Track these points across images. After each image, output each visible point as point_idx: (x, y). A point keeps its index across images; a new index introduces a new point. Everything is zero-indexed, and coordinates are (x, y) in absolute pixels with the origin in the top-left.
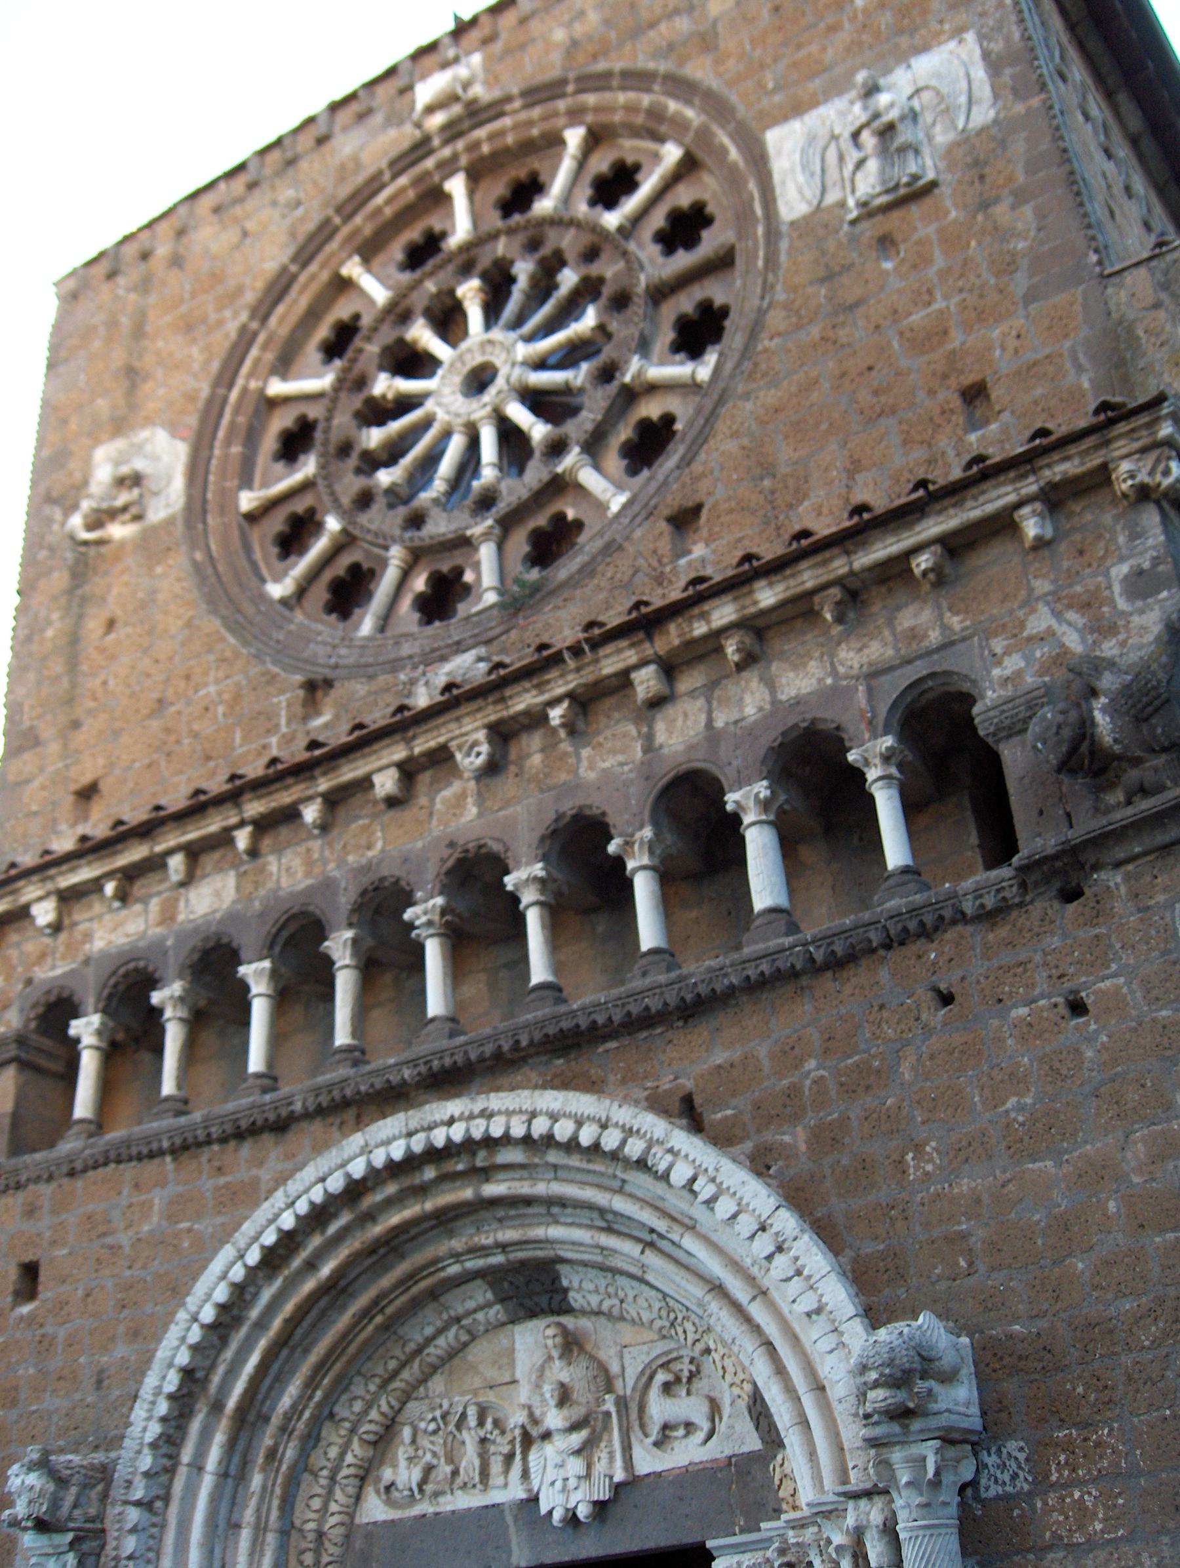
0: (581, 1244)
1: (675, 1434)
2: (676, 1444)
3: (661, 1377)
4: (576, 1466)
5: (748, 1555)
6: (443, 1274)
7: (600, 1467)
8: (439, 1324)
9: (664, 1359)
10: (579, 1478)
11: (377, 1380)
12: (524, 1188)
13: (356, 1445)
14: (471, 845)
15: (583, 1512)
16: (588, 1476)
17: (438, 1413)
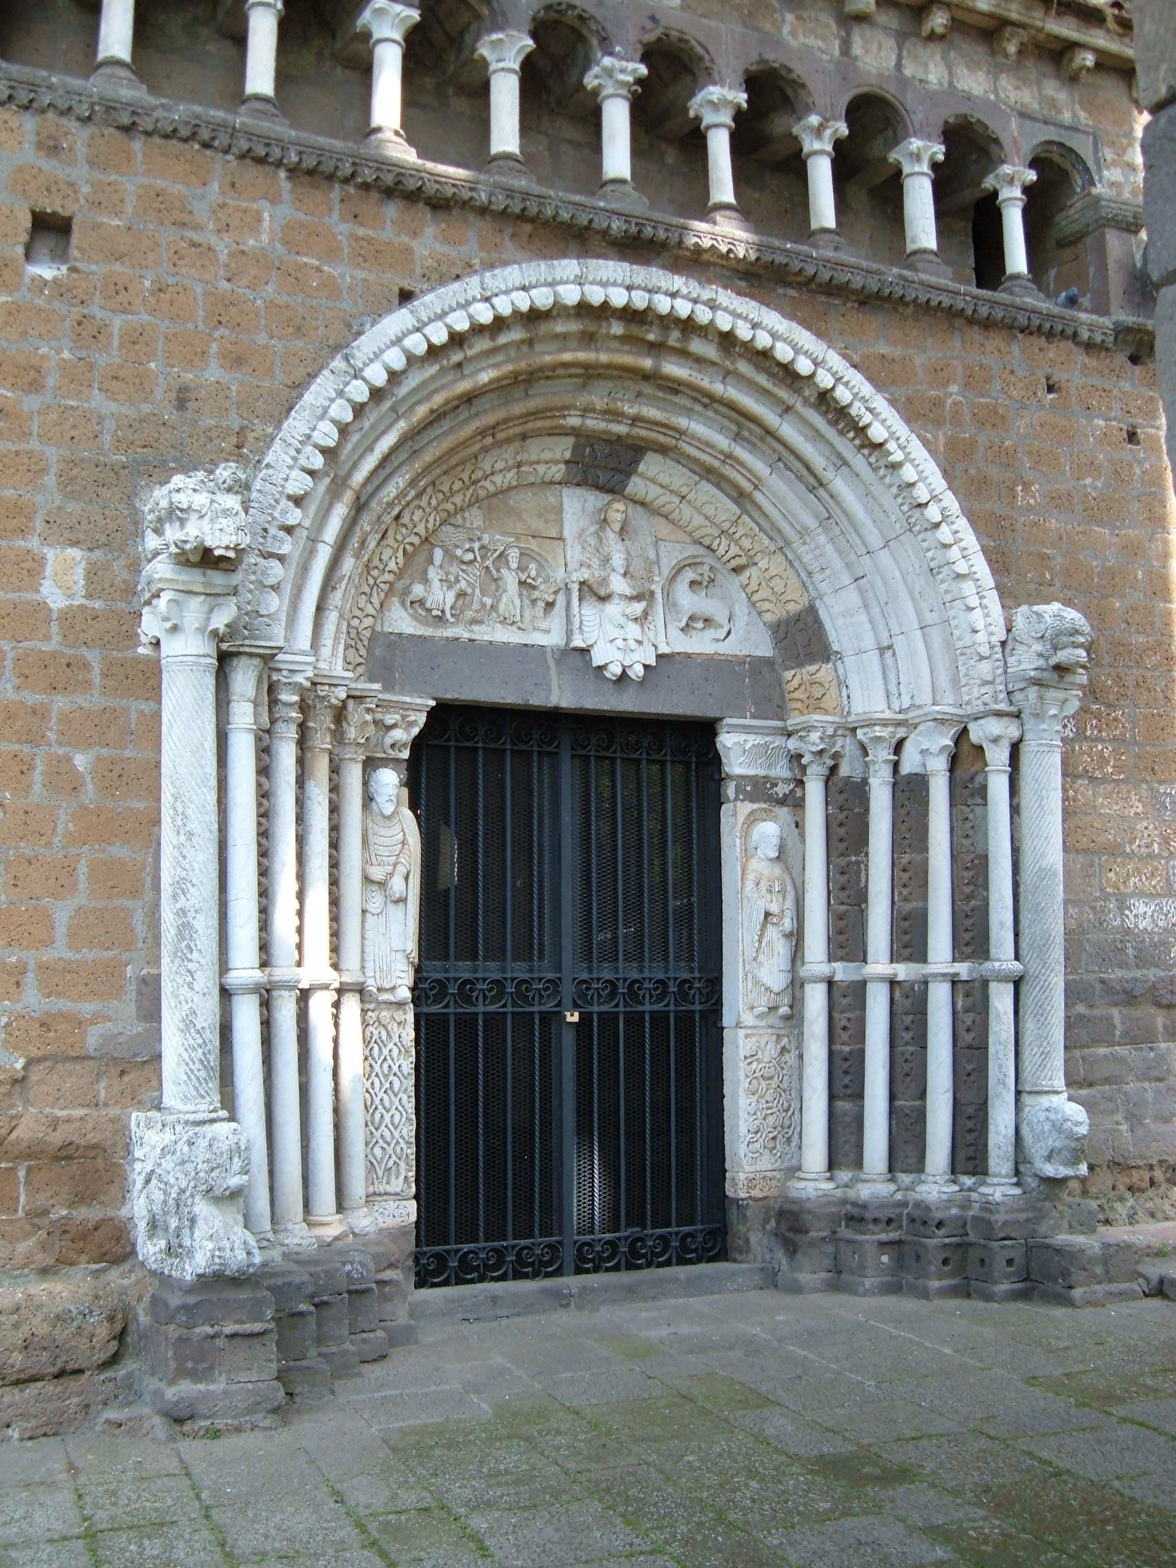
0: (712, 447)
2: (694, 633)
3: (689, 575)
4: (634, 630)
5: (752, 737)
12: (705, 381)
14: (674, 33)
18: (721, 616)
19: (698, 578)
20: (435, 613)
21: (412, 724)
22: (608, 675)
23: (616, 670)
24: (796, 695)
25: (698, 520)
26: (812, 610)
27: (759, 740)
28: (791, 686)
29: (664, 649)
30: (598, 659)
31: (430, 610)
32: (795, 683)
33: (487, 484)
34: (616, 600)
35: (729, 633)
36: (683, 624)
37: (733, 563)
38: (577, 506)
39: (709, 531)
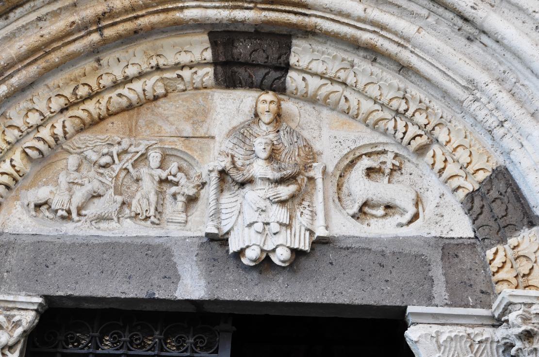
0: (348, 16)
1: (374, 212)
2: (373, 221)
3: (366, 162)
4: (279, 214)
5: (449, 328)
6: (178, 15)
7: (302, 220)
8: (145, 67)
9: (370, 150)
10: (281, 224)
11: (62, 102)
13: (17, 156)
15: (281, 256)
16: (288, 226)
17: (115, 150)
18: (405, 201)
19: (375, 165)
20: (60, 213)
21: (17, 324)
22: (245, 261)
23: (252, 254)
24: (501, 275)
25: (367, 106)
26: (502, 175)
27: (461, 331)
28: (493, 268)
29: (321, 232)
30: (234, 246)
31: (56, 211)
32: (498, 263)
33: (124, 91)
34: (259, 185)
35: (416, 217)
36: (355, 209)
37: (415, 144)
38: (235, 106)
39: (380, 115)
